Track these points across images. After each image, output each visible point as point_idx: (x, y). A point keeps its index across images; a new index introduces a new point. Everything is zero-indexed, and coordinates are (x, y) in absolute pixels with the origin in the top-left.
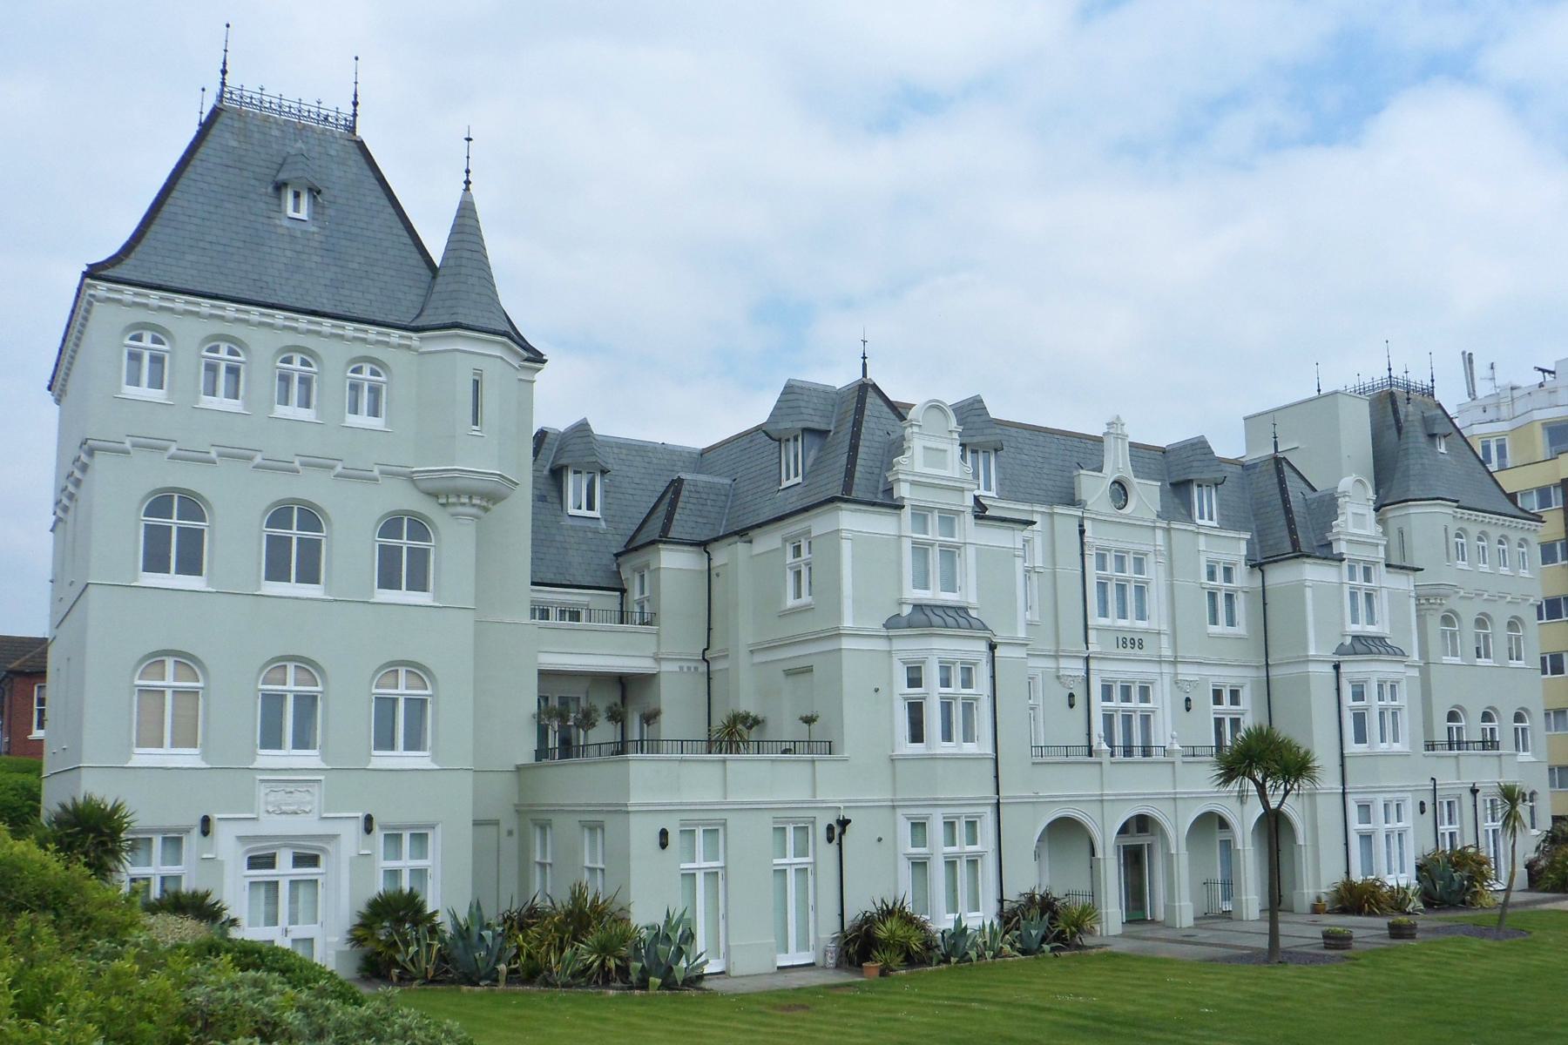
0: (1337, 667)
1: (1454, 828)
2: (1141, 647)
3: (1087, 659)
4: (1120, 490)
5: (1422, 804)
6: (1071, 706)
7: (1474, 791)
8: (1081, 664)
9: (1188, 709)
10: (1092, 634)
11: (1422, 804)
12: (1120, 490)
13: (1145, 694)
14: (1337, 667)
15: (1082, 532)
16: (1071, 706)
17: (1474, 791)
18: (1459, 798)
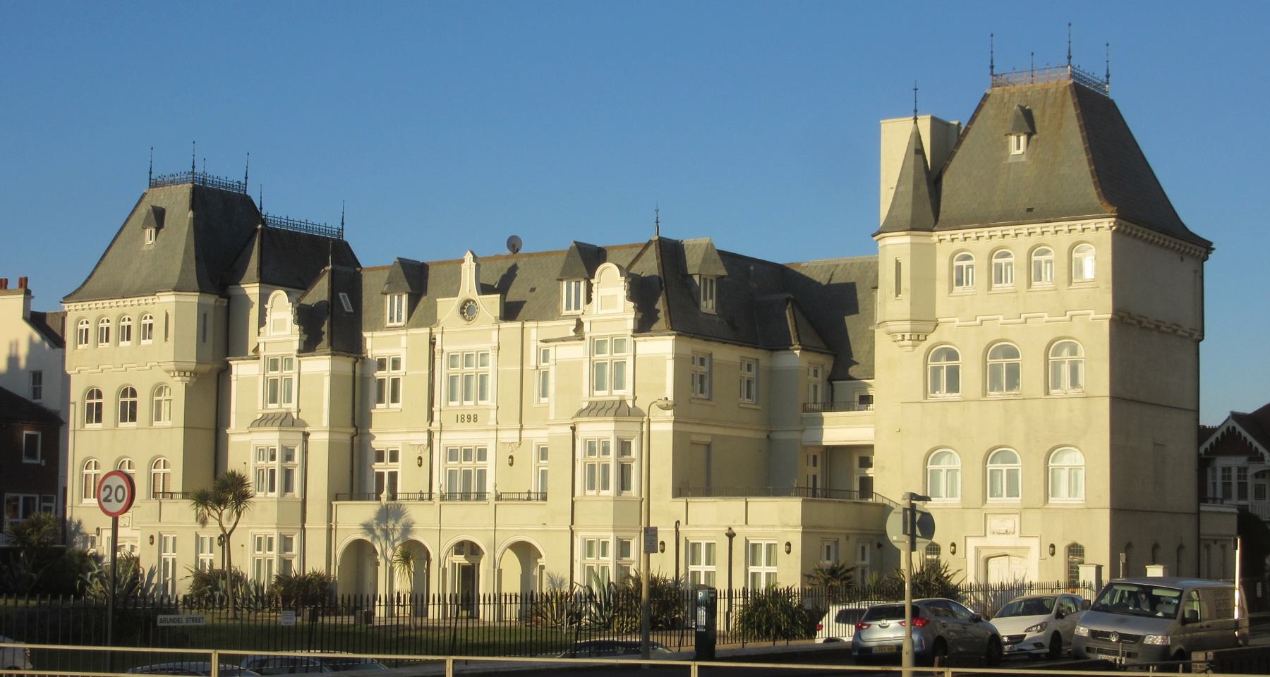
0: (573, 429)
1: (711, 568)
2: (476, 420)
3: (430, 433)
4: (467, 310)
5: (152, 537)
6: (420, 465)
7: (731, 536)
8: (425, 436)
9: (511, 464)
10: (436, 416)
11: (152, 537)
12: (467, 310)
13: (482, 454)
14: (573, 429)
15: (432, 343)
16: (420, 465)
17: (731, 536)
18: (837, 543)
